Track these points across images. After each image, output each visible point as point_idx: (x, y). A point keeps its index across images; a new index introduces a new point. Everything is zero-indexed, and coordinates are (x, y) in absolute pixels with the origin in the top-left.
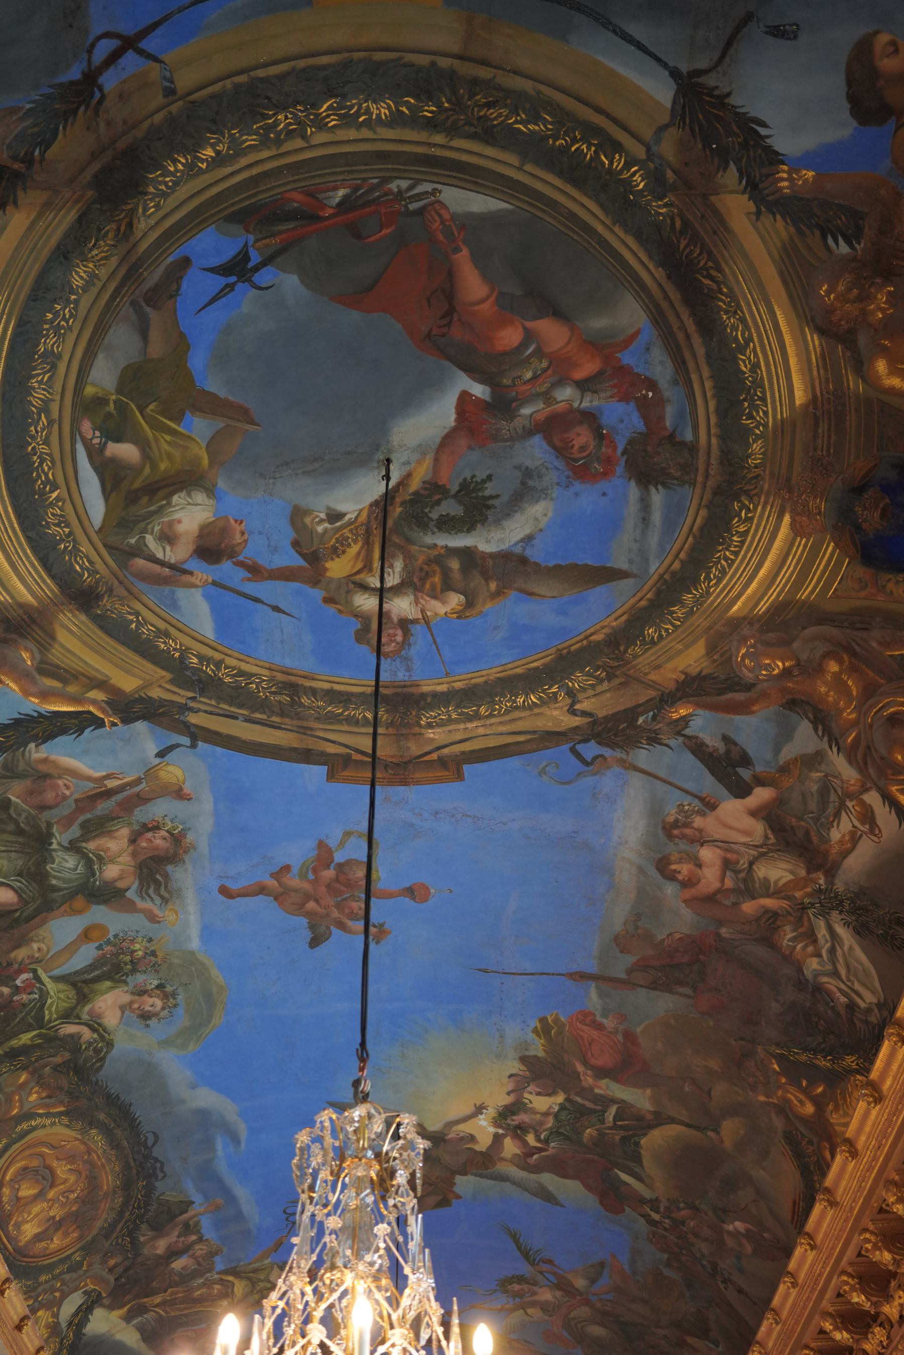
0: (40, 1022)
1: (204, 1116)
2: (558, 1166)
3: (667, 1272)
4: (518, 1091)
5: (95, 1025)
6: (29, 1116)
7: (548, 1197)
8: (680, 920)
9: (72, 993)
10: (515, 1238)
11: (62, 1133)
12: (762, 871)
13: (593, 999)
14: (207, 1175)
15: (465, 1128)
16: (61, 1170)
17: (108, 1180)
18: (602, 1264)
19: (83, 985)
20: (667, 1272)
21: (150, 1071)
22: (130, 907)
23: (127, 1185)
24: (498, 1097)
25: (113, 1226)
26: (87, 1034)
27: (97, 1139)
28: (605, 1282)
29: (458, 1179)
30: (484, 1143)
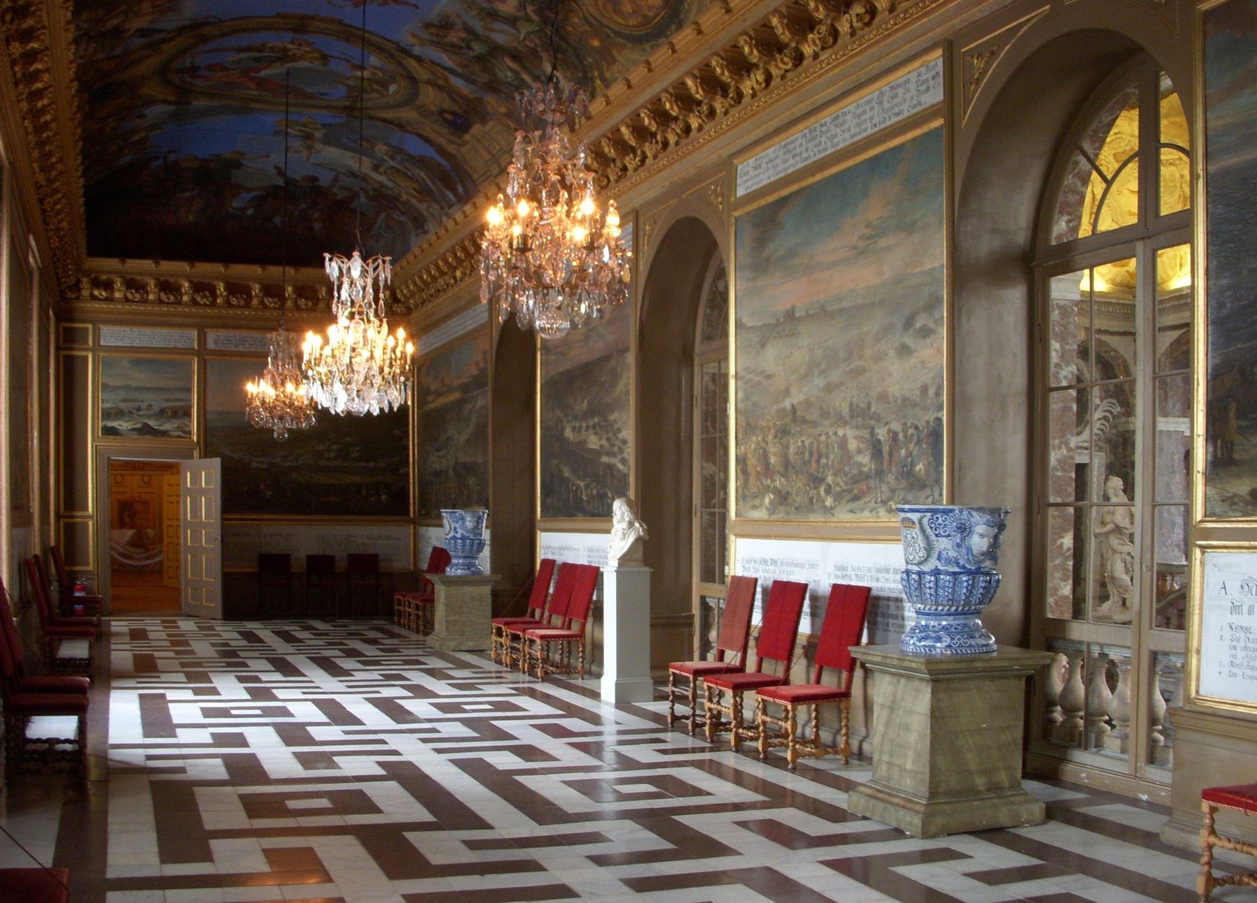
0: (540, 31)
6: (585, 18)
9: (518, 24)
12: (120, 19)
19: (513, 21)
22: (464, 24)
26: (530, 9)
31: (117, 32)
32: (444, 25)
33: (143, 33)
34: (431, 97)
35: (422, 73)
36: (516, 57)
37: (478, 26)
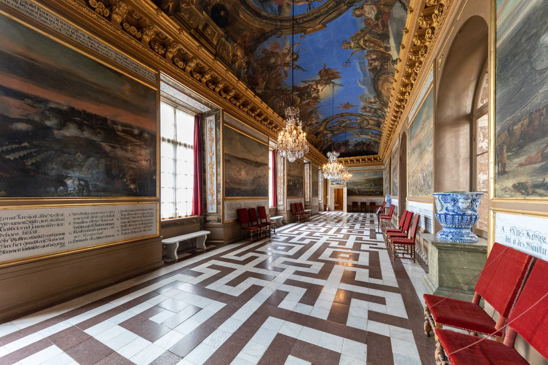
1: (364, 85)
2: (307, 88)
3: (280, 87)
4: (318, 95)
5: (375, 99)
7: (305, 82)
8: (313, 115)
10: (304, 70)
11: (383, 92)
13: (316, 107)
14: (365, 75)
15: (322, 87)
16: (386, 88)
17: (380, 82)
18: (287, 76)
19: (375, 103)
20: (280, 87)
21: (370, 93)
23: (378, 79)
24: (320, 93)
25: (383, 74)
27: (380, 89)
28: (283, 74)
29: (320, 78)
30: (319, 86)
31: (311, 124)
32: (365, 108)
33: (317, 123)
34: (371, 122)
35: (368, 118)
36: (380, 110)
37: (370, 106)
